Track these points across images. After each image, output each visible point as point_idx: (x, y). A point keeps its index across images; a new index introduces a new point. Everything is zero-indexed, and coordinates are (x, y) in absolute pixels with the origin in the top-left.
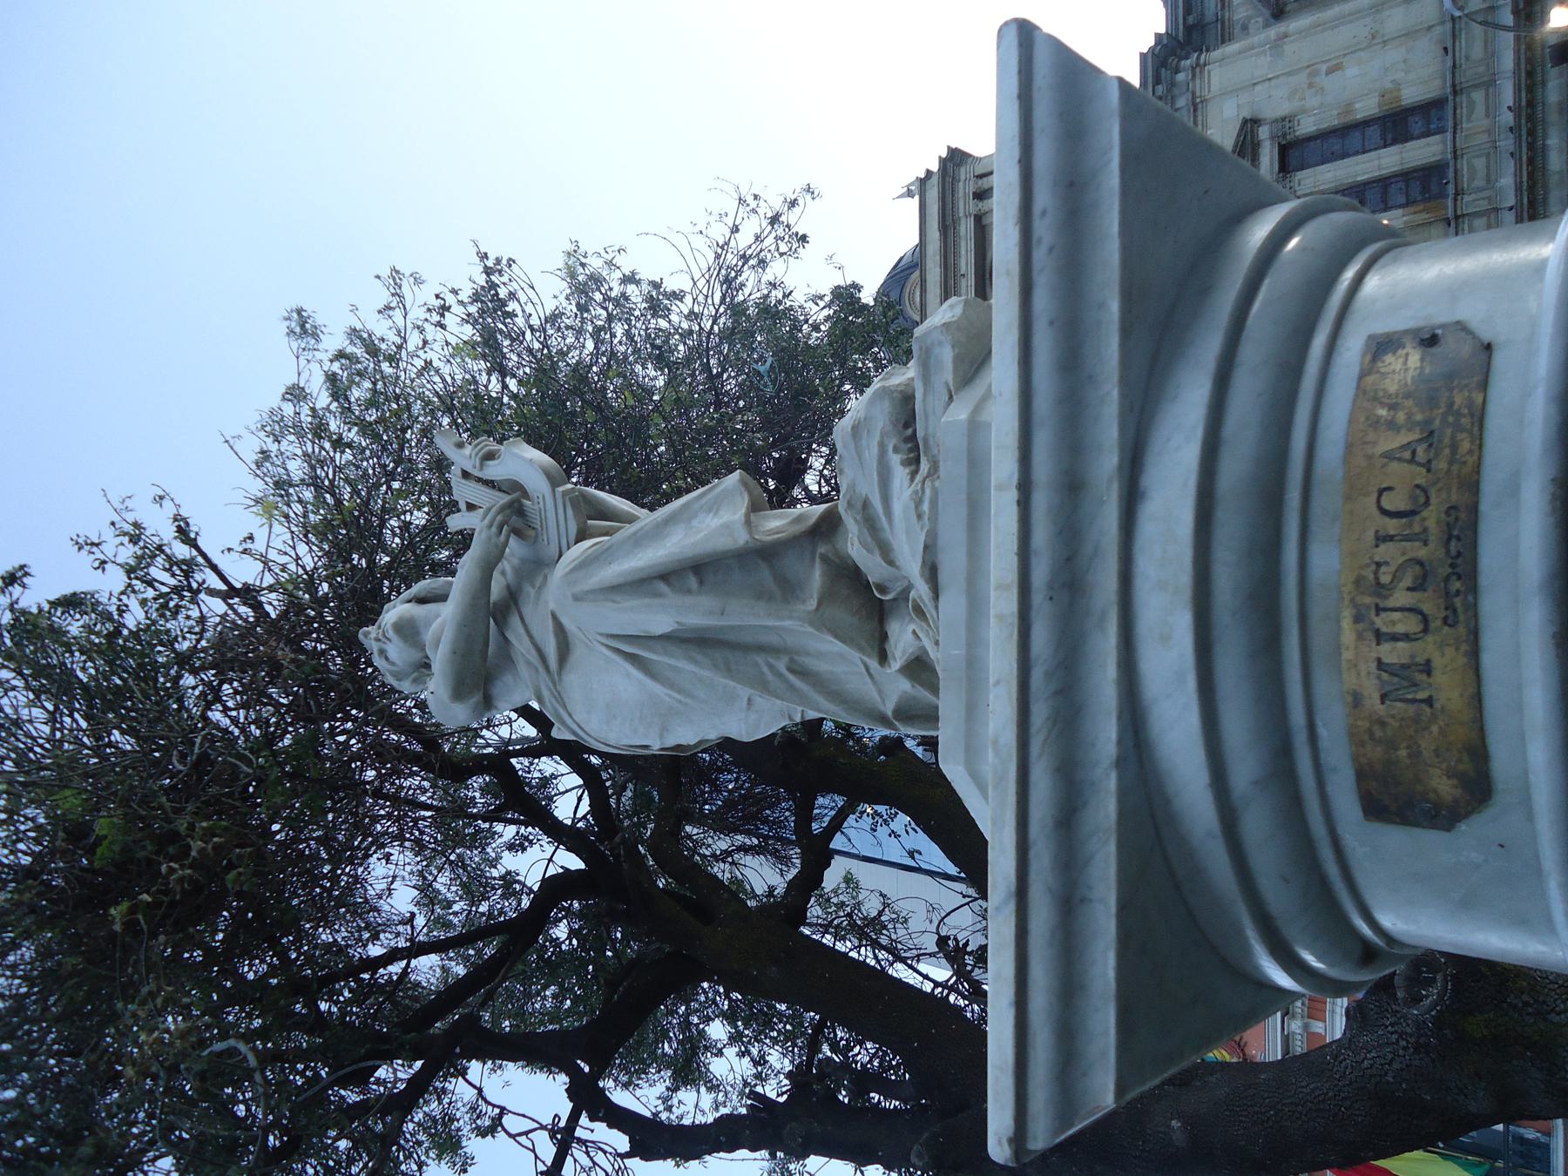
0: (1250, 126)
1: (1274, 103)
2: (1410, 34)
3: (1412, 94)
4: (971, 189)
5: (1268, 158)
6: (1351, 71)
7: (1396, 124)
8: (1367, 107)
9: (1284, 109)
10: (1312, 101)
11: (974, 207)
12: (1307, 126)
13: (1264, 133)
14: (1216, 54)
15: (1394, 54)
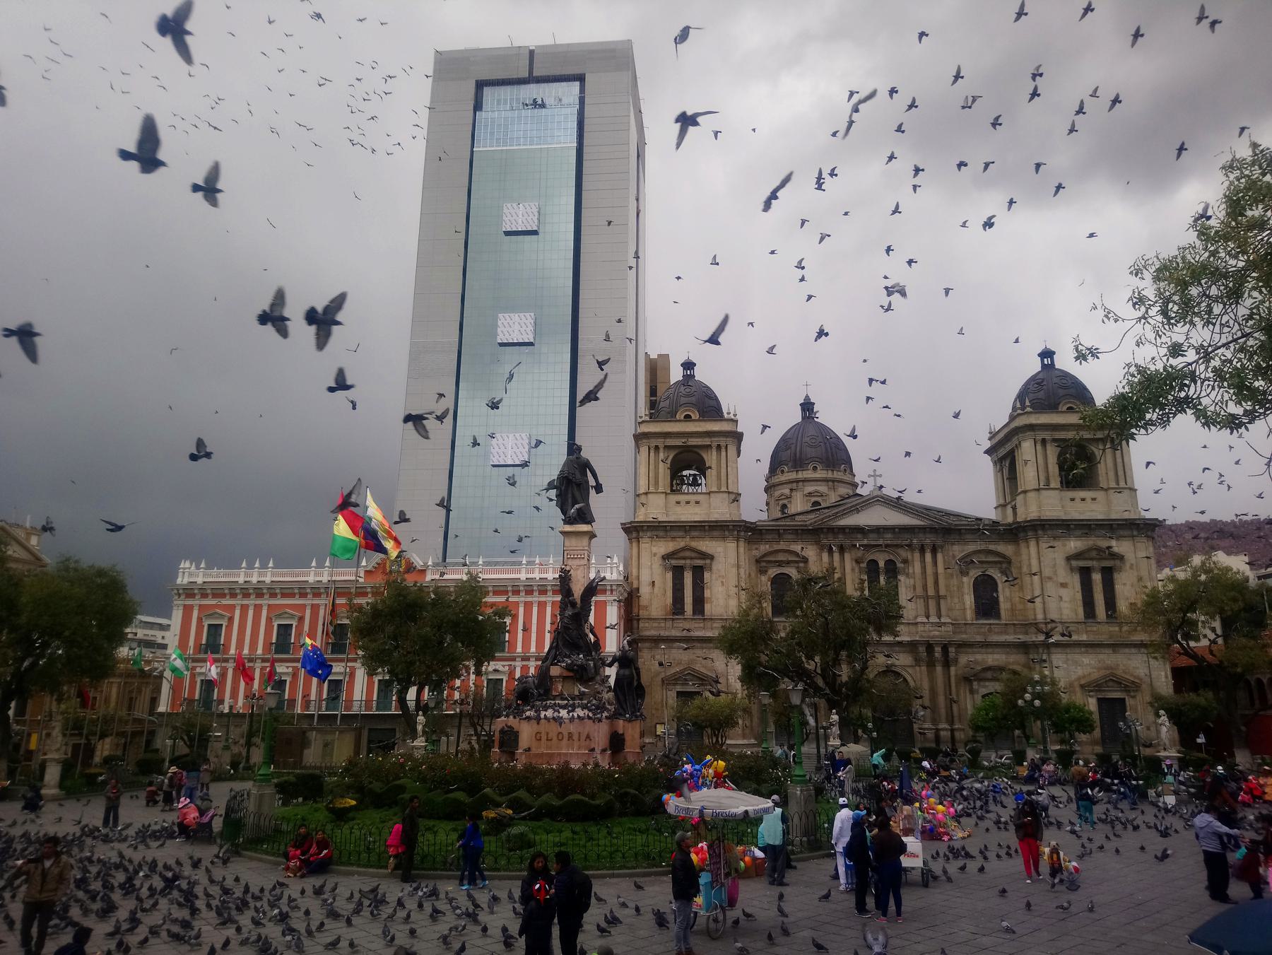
0: (712, 558)
1: (718, 566)
2: (727, 606)
3: (707, 607)
4: (723, 444)
5: (699, 562)
6: (720, 589)
7: (699, 602)
8: (707, 594)
9: (714, 567)
10: (714, 577)
11: (714, 445)
12: (707, 575)
13: (708, 561)
14: (742, 544)
15: (722, 602)
